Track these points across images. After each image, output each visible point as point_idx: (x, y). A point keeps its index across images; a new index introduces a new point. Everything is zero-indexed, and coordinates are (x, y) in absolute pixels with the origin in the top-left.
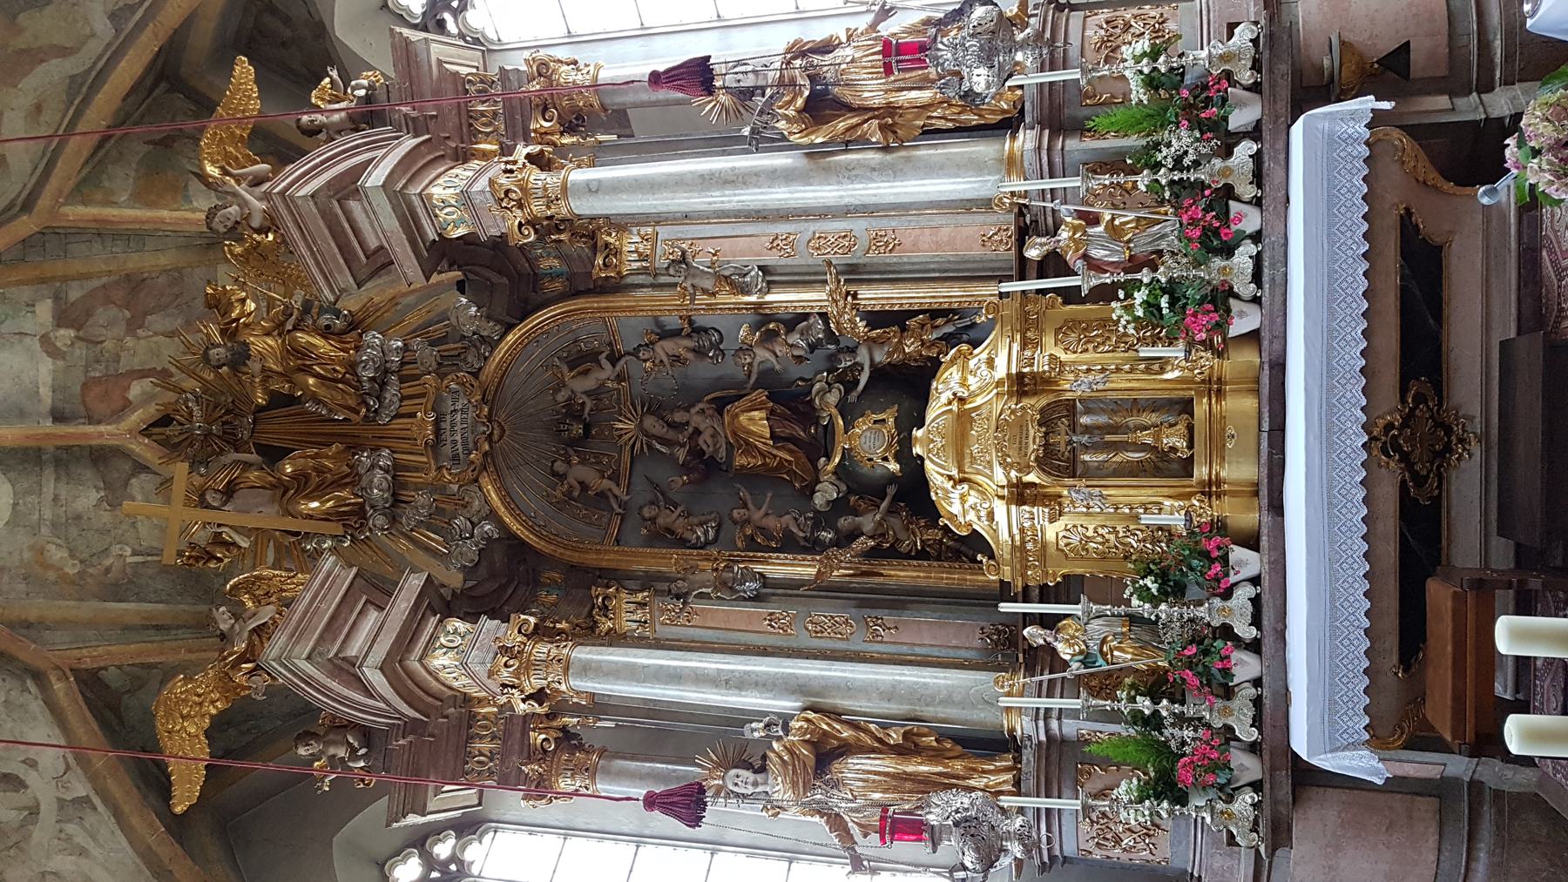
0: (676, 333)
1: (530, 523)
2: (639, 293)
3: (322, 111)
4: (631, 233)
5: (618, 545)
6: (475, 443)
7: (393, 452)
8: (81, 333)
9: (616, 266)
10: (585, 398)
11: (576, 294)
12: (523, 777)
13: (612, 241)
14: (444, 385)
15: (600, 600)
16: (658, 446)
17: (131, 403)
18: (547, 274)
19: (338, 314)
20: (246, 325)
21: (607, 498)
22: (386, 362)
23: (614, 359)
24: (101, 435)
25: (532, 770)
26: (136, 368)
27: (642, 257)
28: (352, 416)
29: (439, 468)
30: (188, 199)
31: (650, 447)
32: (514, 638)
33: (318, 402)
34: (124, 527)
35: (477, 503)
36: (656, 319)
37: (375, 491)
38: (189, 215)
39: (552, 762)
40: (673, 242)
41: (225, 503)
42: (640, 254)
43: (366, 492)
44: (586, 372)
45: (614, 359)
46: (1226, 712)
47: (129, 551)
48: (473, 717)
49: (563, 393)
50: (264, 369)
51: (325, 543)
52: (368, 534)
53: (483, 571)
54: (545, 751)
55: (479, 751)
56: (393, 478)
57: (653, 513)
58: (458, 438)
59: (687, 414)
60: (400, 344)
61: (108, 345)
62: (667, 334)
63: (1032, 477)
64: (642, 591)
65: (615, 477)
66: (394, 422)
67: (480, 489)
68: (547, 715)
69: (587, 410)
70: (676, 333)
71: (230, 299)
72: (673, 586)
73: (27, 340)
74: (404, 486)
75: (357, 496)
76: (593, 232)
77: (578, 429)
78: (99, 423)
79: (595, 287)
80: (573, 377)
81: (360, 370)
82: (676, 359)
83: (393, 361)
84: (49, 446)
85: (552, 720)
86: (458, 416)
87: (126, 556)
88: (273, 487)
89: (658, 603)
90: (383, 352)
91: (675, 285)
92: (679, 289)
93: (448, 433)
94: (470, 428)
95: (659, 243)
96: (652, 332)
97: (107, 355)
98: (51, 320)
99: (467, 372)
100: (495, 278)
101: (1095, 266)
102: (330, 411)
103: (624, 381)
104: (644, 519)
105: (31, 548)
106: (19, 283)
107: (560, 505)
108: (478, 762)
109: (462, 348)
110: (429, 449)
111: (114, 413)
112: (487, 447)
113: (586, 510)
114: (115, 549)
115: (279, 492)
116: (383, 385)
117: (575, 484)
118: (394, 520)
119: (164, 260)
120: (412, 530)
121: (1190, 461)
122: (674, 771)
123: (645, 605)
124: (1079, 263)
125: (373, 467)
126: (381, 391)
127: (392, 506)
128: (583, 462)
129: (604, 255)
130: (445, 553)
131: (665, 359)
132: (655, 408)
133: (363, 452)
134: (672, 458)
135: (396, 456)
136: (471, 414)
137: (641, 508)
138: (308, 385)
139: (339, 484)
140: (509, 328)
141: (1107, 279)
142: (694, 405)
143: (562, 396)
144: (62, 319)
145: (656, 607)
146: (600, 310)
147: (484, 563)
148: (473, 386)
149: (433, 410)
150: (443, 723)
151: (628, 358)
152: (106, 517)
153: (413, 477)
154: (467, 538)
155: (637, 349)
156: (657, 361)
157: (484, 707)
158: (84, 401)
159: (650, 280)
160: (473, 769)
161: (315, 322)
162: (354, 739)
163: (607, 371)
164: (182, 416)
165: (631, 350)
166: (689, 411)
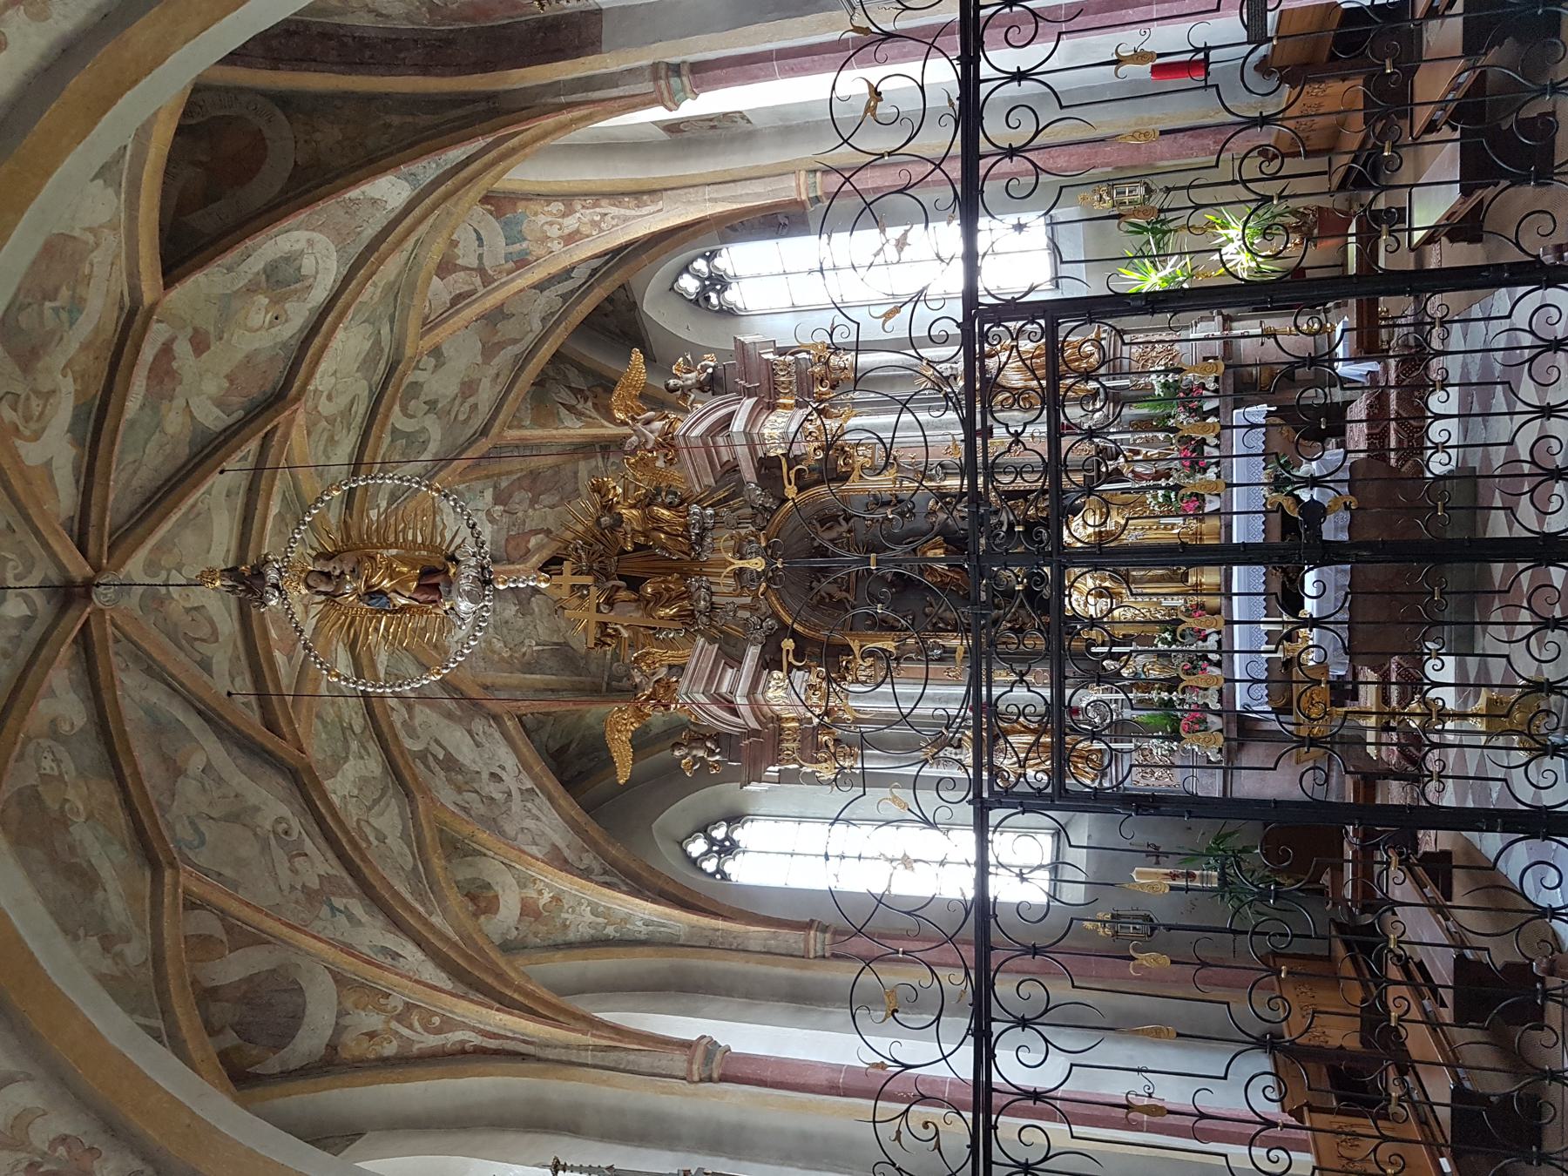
3: (679, 378)
20: (618, 503)
23: (847, 520)
33: (663, 548)
38: (566, 432)
45: (847, 520)
46: (1205, 697)
50: (633, 529)
61: (520, 514)
63: (1107, 584)
78: (513, 563)
88: (636, 601)
101: (1138, 476)
106: (477, 479)
114: (527, 642)
119: (550, 460)
124: (1130, 476)
139: (680, 597)
141: (1144, 484)
144: (497, 500)
152: (520, 622)
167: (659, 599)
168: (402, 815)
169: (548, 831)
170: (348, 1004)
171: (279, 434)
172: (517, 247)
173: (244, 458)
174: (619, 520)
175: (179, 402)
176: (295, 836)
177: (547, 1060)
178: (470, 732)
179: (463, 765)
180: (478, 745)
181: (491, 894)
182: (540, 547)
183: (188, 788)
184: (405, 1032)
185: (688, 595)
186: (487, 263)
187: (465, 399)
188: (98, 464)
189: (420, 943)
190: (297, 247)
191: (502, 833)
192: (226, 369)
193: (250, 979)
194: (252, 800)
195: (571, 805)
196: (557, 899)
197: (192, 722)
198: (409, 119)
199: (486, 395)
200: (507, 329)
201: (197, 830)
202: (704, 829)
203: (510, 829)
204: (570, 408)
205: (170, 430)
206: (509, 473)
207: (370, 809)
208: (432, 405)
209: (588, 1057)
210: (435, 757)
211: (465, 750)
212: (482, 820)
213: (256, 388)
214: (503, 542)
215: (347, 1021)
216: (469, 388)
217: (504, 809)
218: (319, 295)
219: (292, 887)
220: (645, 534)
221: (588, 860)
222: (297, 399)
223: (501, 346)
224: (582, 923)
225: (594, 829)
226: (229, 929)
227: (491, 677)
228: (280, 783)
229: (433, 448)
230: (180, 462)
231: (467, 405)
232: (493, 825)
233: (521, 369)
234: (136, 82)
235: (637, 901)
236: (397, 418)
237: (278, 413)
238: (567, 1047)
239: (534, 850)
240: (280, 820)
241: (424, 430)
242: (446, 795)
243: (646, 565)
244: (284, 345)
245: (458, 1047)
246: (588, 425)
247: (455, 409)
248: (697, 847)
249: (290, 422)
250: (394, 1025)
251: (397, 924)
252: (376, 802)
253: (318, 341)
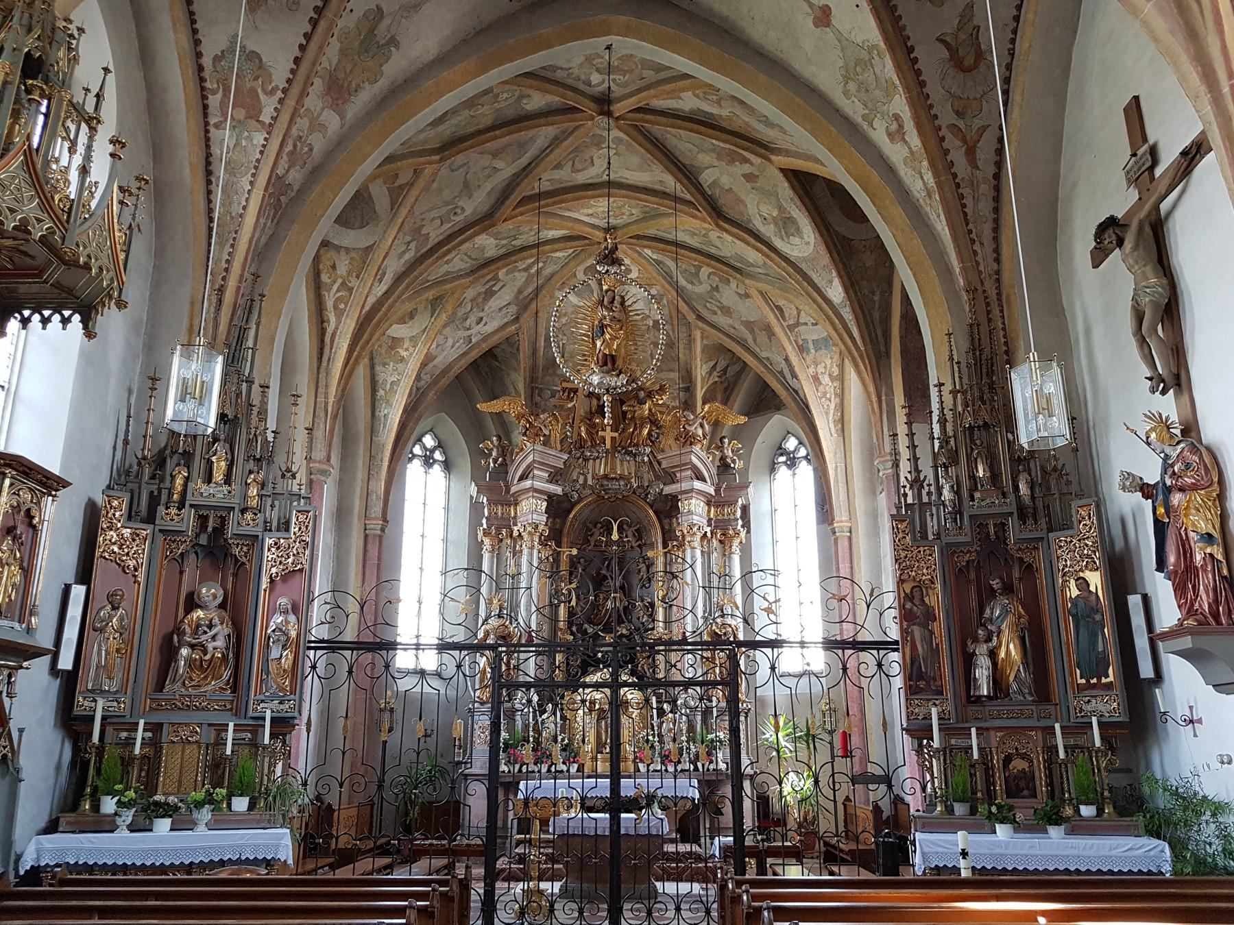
3: (729, 444)
23: (639, 546)
30: (706, 362)
32: (541, 528)
38: (699, 366)
45: (639, 546)
50: (635, 411)
65: (595, 545)
101: (660, 727)
121: (602, 753)
139: (593, 440)
168: (461, 270)
169: (445, 353)
170: (353, 254)
171: (697, 213)
172: (811, 346)
173: (683, 192)
174: (642, 402)
175: (716, 163)
176: (453, 218)
177: (318, 373)
178: (509, 304)
180: (500, 309)
181: (407, 320)
183: (486, 161)
184: (335, 287)
186: (802, 328)
188: (680, 121)
189: (387, 294)
190: (805, 236)
191: (445, 326)
192: (734, 189)
193: (370, 198)
194: (476, 194)
196: (402, 360)
197: (524, 161)
198: (877, 305)
199: (722, 320)
200: (762, 337)
201: (461, 166)
202: (440, 446)
203: (448, 330)
204: (714, 367)
205: (700, 156)
207: (466, 254)
208: (717, 289)
209: (321, 399)
210: (494, 285)
211: (498, 302)
212: (454, 314)
213: (724, 202)
215: (343, 252)
216: (727, 311)
218: (778, 243)
219: (423, 219)
220: (633, 417)
221: (426, 378)
222: (717, 225)
223: (752, 332)
224: (387, 375)
225: (444, 382)
226: (401, 187)
228: (486, 207)
230: (680, 158)
232: (451, 320)
233: (738, 343)
234: (874, 205)
235: (401, 411)
236: (705, 271)
237: (710, 215)
238: (327, 386)
239: (434, 346)
240: (463, 209)
241: (701, 283)
242: (470, 293)
244: (750, 221)
245: (326, 318)
246: (703, 379)
248: (429, 441)
249: (704, 220)
250: (340, 281)
251: (398, 279)
252: (470, 257)
253: (752, 241)
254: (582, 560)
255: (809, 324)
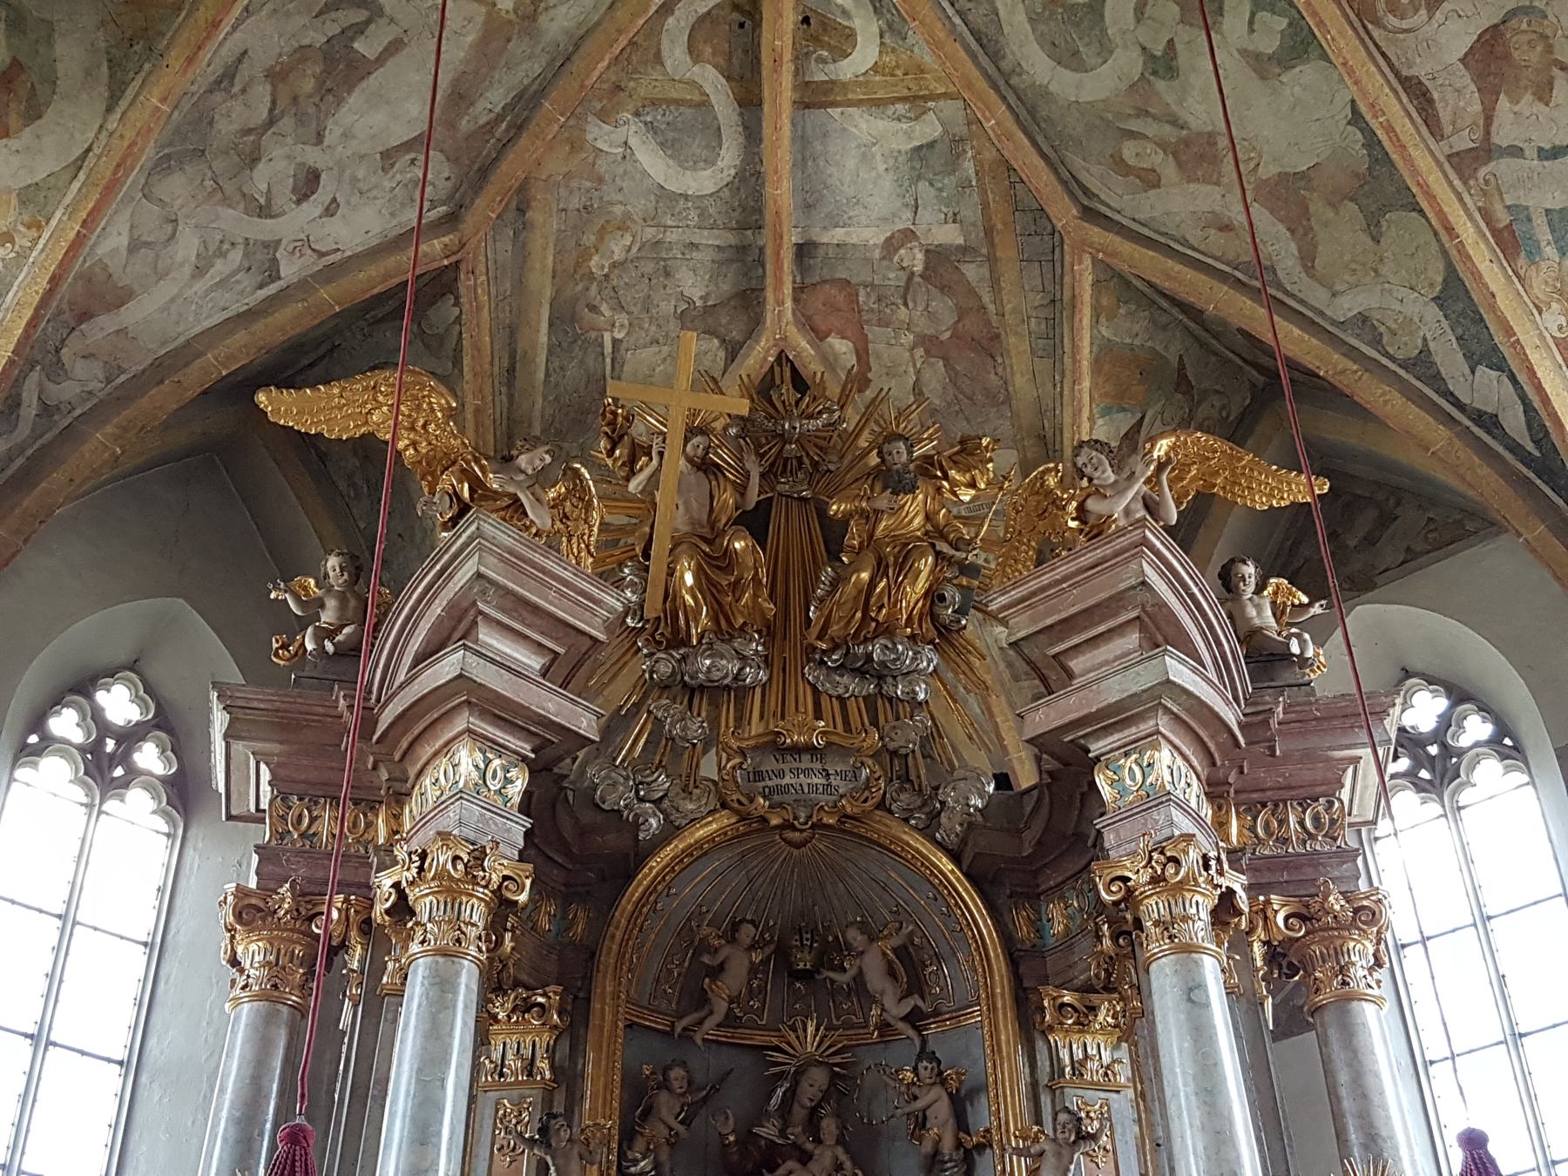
0: (962, 1124)
1: (659, 888)
2: (1021, 1061)
4: (1116, 1047)
5: (626, 1026)
6: (781, 805)
7: (764, 685)
8: (917, 279)
9: (1061, 1023)
10: (852, 972)
11: (1014, 959)
12: (272, 885)
13: (1100, 1018)
14: (865, 759)
15: (540, 1000)
16: (780, 1092)
17: (822, 339)
18: (1039, 914)
19: (962, 611)
20: (939, 489)
21: (696, 1010)
22: (894, 678)
24: (781, 303)
25: (283, 900)
26: (870, 346)
27: (1078, 1067)
28: (815, 630)
29: (742, 752)
31: (780, 1076)
33: (835, 584)
34: (653, 328)
35: (691, 807)
36: (979, 1089)
37: (708, 662)
39: (292, 930)
40: (1106, 1118)
41: (690, 460)
42: (1082, 1063)
43: (705, 651)
44: (892, 973)
47: (619, 336)
48: (373, 806)
49: (859, 938)
51: (633, 592)
52: (645, 651)
53: (587, 817)
54: (311, 919)
55: (317, 818)
56: (727, 686)
57: (676, 1085)
58: (787, 780)
59: (833, 1142)
60: (922, 696)
62: (960, 1105)
64: (552, 1068)
66: (808, 687)
67: (711, 813)
68: (368, 921)
69: (832, 975)
70: (962, 1124)
71: (975, 468)
72: (561, 1121)
73: (909, 214)
74: (715, 705)
75: (701, 637)
76: (1114, 990)
77: (804, 961)
78: (796, 300)
79: (1025, 989)
80: (884, 954)
81: (882, 641)
82: (921, 1122)
83: (897, 687)
84: (766, 239)
85: (360, 929)
86: (819, 780)
87: (612, 332)
88: (712, 524)
89: (533, 1096)
90: (908, 673)
91: (1039, 1122)
92: (1035, 1128)
93: (795, 765)
94: (804, 797)
95: (1102, 1095)
96: (961, 1082)
97: (888, 311)
98: (936, 243)
99: (885, 793)
100: (1030, 837)
102: (822, 600)
103: (880, 1035)
104: (666, 1070)
105: (627, 216)
106: (985, 205)
107: (686, 932)
108: (300, 816)
109: (920, 785)
110: (770, 738)
111: (809, 318)
112: (775, 821)
113: (679, 975)
114: (622, 318)
115: (706, 532)
116: (861, 673)
117: (720, 958)
118: (665, 687)
120: (650, 712)
122: (261, 1134)
123: (530, 1074)
125: (743, 658)
126: (852, 670)
127: (685, 684)
128: (753, 970)
129: (1076, 1004)
130: (615, 759)
131: (920, 1104)
132: (842, 1085)
133: (763, 645)
134: (761, 1115)
135: (758, 691)
136: (824, 799)
137: (684, 1064)
138: (858, 571)
140: (955, 858)
142: (847, 1151)
143: (855, 937)
145: (528, 1092)
146: (991, 997)
147: (599, 818)
148: (865, 801)
149: (829, 744)
150: (365, 764)
151: (917, 1042)
152: (667, 307)
153: (728, 714)
154: (637, 792)
155: (933, 1057)
156: (914, 1090)
157: (387, 822)
158: (825, 282)
159: (1044, 1079)
160: (290, 808)
161: (949, 581)
162: (349, 636)
163: (897, 1009)
164: (807, 406)
165: (931, 1046)
166: (838, 1142)
167: (716, 563)
169: (167, 290)
172: (1544, 234)
179: (340, 102)
180: (389, 157)
182: (829, 361)
185: (725, 630)
186: (1502, 167)
187: (1174, 151)
195: (231, 358)
206: (995, 283)
208: (1164, 64)
210: (360, 29)
211: (378, 118)
212: (202, 120)
214: (841, 274)
217: (229, 187)
223: (1299, 224)
225: (163, 399)
227: (546, 223)
229: (1063, 84)
231: (1157, 159)
243: (795, 555)
247: (1151, 128)
254: (677, 1073)
255: (1531, 152)
